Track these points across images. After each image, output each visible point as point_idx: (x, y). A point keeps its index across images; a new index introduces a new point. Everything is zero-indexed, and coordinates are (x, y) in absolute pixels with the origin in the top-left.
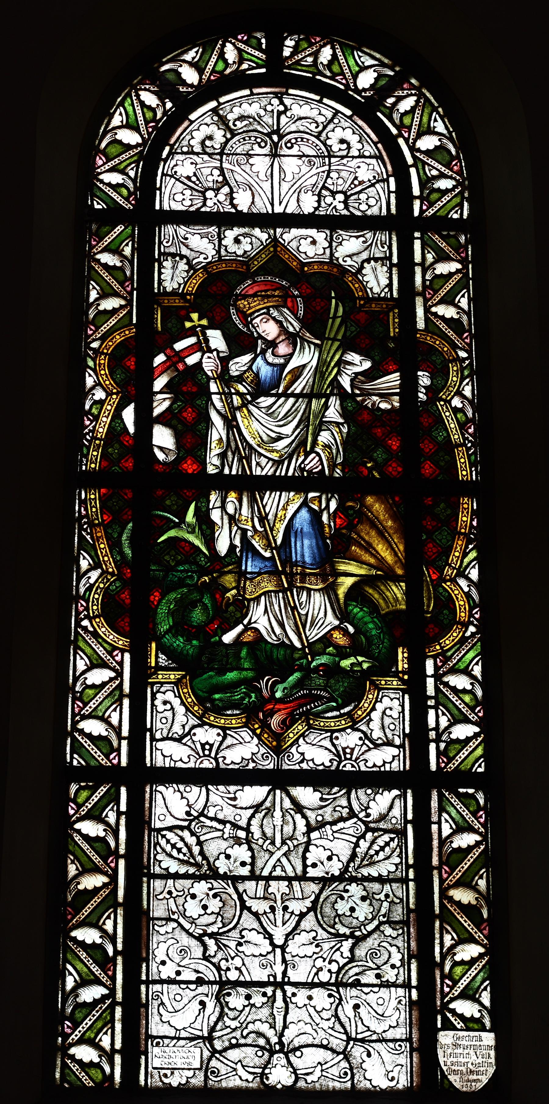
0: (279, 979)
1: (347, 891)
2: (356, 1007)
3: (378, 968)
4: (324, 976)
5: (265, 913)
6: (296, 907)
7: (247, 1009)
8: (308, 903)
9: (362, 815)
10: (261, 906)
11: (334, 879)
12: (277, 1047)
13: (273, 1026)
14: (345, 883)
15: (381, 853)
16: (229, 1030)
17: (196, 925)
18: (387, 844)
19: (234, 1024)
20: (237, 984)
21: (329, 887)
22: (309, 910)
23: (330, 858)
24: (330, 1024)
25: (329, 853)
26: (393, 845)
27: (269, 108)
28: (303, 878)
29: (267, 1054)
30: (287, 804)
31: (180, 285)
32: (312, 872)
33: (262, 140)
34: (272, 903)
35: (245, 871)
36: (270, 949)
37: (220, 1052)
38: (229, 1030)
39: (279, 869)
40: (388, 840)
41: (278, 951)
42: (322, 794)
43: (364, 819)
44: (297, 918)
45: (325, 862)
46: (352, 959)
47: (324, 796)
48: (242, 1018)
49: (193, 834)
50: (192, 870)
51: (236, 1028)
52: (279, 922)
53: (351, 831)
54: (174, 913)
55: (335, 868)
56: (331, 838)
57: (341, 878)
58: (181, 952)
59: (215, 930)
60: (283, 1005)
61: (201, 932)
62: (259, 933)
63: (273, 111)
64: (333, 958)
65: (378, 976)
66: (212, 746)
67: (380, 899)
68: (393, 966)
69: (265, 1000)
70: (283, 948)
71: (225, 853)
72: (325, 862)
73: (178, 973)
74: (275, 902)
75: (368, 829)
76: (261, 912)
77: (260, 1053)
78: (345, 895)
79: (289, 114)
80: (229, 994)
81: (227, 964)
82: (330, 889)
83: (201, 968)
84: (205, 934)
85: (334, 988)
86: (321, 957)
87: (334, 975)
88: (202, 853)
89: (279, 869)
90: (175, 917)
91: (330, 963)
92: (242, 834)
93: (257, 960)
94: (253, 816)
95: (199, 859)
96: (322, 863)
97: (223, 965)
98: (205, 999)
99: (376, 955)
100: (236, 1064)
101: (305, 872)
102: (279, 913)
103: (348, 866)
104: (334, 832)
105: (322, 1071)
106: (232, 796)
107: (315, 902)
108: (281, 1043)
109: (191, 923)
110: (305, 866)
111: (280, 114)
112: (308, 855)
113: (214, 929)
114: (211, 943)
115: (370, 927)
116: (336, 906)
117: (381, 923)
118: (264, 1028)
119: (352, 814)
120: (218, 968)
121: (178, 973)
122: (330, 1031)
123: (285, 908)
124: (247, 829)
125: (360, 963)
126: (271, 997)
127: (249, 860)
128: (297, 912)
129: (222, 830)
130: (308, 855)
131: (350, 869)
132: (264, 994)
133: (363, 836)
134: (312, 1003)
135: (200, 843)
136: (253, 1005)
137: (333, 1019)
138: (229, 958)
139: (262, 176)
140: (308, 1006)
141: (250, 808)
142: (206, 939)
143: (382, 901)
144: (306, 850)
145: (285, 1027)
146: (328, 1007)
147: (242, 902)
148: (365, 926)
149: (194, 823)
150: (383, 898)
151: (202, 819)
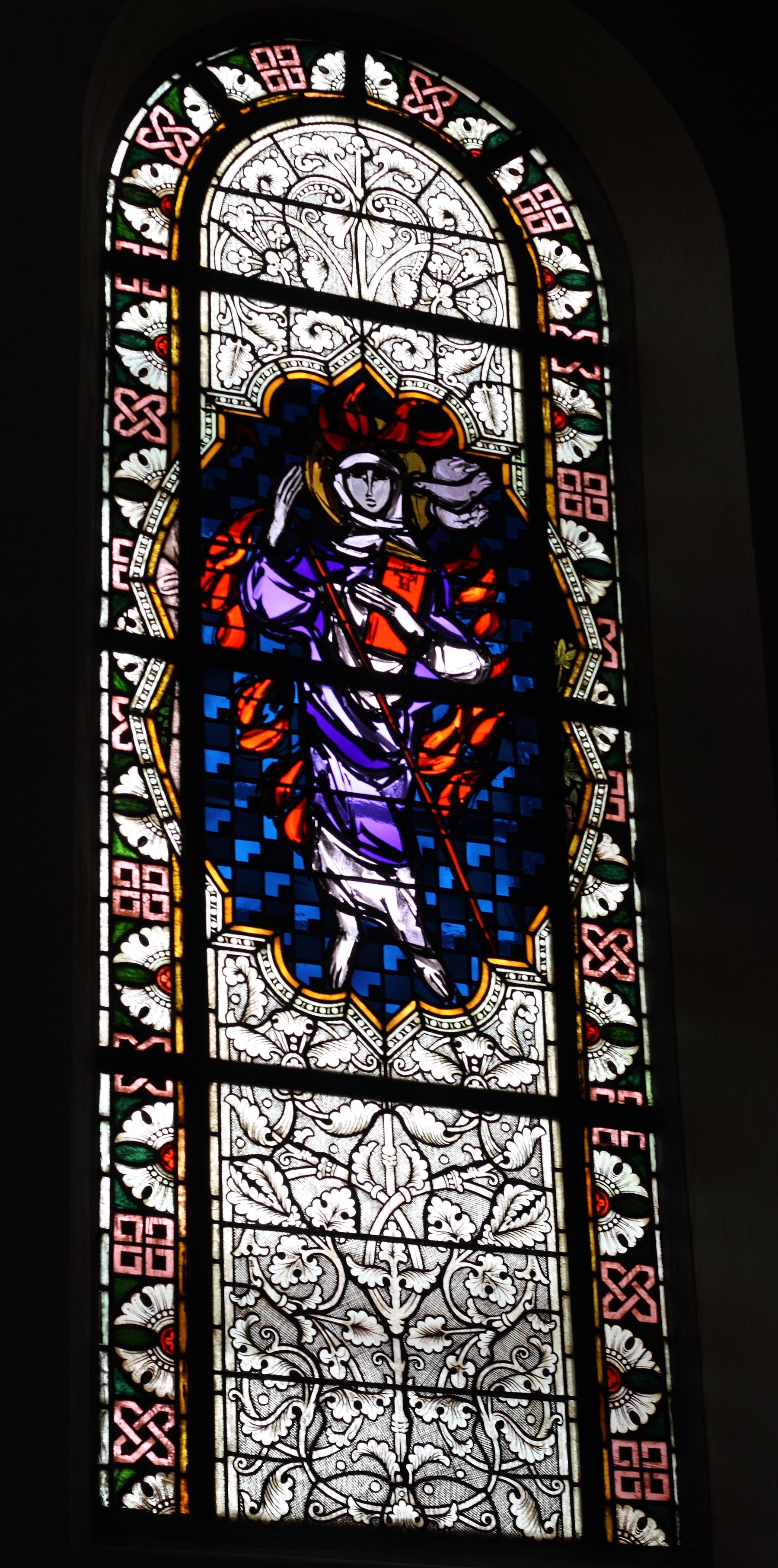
0: (399, 1380)
2: (499, 1425)
3: (529, 1372)
4: (458, 1381)
5: (377, 1286)
6: (419, 1283)
7: (358, 1421)
8: (432, 1277)
9: (498, 1160)
10: (372, 1277)
11: (463, 1245)
12: (399, 1479)
14: (480, 1252)
15: (525, 1215)
16: (334, 1449)
17: (288, 1297)
18: (533, 1204)
19: (341, 1440)
20: (343, 1385)
21: (459, 1255)
22: (434, 1287)
23: (458, 1217)
24: (466, 1449)
25: (457, 1210)
26: (540, 1205)
27: (350, 149)
28: (424, 1242)
29: (386, 1487)
31: (243, 380)
32: (435, 1235)
34: (388, 1276)
35: (347, 1226)
36: (385, 1338)
37: (325, 1481)
38: (334, 1449)
39: (392, 1225)
40: (532, 1198)
41: (396, 1343)
42: (447, 1126)
45: (453, 1220)
46: (491, 1360)
48: (352, 1432)
49: (278, 1168)
50: (276, 1220)
51: (344, 1446)
52: (396, 1303)
53: (484, 1182)
54: (256, 1278)
55: (465, 1229)
57: (473, 1245)
58: (266, 1333)
60: (405, 1420)
61: (294, 1308)
62: (369, 1314)
64: (470, 1357)
65: (527, 1384)
67: (523, 1279)
68: (546, 1372)
69: (380, 1410)
71: (320, 1198)
72: (453, 1220)
74: (389, 1272)
75: (508, 1181)
76: (372, 1285)
80: (332, 1400)
81: (330, 1356)
83: (297, 1360)
84: (299, 1311)
85: (469, 1398)
87: (470, 1379)
89: (392, 1225)
90: (258, 1283)
91: (465, 1361)
93: (368, 1353)
94: (356, 1149)
95: (287, 1203)
96: (447, 1222)
97: (325, 1356)
98: (300, 1405)
99: (524, 1354)
100: (347, 1497)
101: (427, 1233)
102: (395, 1288)
103: (483, 1229)
104: (464, 1181)
105: (459, 1513)
106: (326, 1117)
107: (440, 1278)
108: (403, 1472)
109: (281, 1294)
110: (426, 1224)
111: (364, 160)
112: (430, 1208)
113: (310, 1304)
114: (307, 1324)
115: (513, 1316)
118: (381, 1450)
120: (318, 1361)
121: (264, 1364)
123: (402, 1283)
124: (348, 1167)
126: (388, 1407)
127: (352, 1212)
129: (316, 1166)
130: (430, 1208)
131: (485, 1234)
132: (380, 1403)
133: (500, 1189)
135: (286, 1182)
137: (470, 1442)
138: (332, 1349)
139: (339, 242)
141: (355, 1134)
142: (301, 1318)
144: (428, 1203)
146: (464, 1425)
147: (347, 1269)
149: (278, 1152)
150: (528, 1277)
151: (288, 1146)
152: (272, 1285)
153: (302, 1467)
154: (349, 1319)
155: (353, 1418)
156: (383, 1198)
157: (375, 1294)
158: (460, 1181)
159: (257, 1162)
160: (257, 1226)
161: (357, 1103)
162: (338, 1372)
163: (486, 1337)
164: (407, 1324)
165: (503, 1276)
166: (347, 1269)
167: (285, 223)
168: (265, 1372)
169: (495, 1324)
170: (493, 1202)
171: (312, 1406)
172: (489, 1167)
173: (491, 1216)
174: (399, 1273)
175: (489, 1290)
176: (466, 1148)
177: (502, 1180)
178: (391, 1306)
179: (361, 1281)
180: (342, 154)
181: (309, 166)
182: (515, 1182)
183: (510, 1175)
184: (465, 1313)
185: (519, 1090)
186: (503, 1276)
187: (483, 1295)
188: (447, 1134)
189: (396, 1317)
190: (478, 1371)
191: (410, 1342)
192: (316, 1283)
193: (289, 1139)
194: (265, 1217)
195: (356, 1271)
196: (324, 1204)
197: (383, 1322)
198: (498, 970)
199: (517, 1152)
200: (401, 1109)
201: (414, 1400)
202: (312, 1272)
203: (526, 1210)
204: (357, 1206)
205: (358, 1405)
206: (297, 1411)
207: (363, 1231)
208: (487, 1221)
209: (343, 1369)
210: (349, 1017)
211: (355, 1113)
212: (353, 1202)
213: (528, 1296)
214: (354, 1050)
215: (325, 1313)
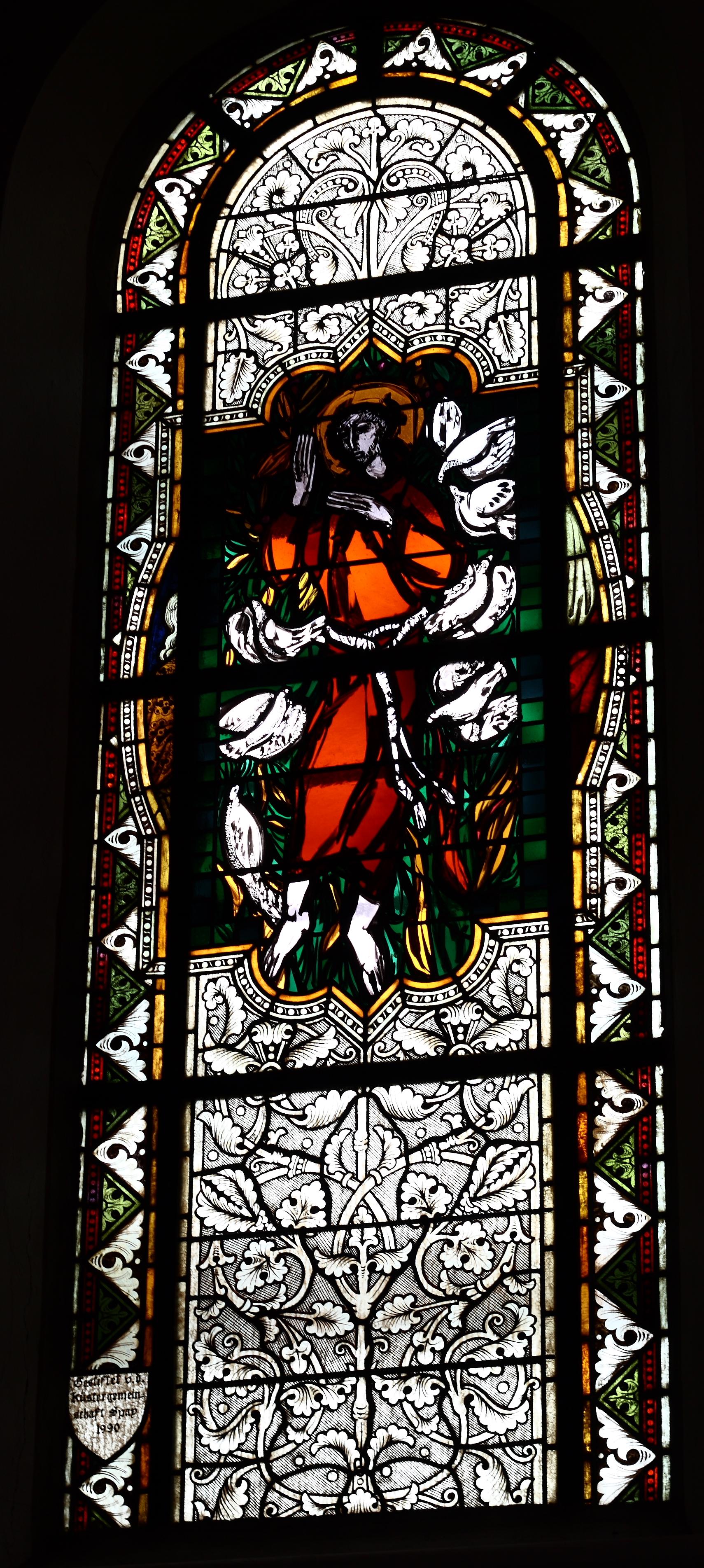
0: (361, 1366)
1: (457, 1233)
2: (468, 1400)
4: (426, 1358)
6: (387, 1263)
7: (318, 1414)
8: (404, 1256)
11: (439, 1218)
13: (352, 1436)
14: (455, 1223)
18: (516, 1161)
21: (434, 1229)
22: (404, 1265)
23: (433, 1190)
25: (433, 1183)
26: (524, 1162)
30: (376, 1116)
33: (350, 180)
35: (319, 1220)
36: (351, 1326)
40: (517, 1156)
41: (361, 1329)
43: (485, 1128)
44: (387, 1279)
46: (463, 1331)
47: (428, 1101)
49: (249, 1174)
50: (243, 1227)
53: (463, 1149)
55: (441, 1202)
56: (438, 1161)
59: (276, 1306)
63: (370, 136)
65: (500, 1351)
66: (277, 1047)
68: (522, 1336)
69: (342, 1398)
70: (367, 1323)
73: (226, 1372)
74: (358, 1259)
75: (490, 1143)
76: (338, 1274)
77: (333, 1476)
78: (455, 1239)
79: (393, 135)
82: (438, 1230)
86: (421, 1330)
88: (260, 1200)
92: (314, 1167)
95: (256, 1208)
97: (286, 1353)
99: (498, 1320)
100: (301, 1494)
107: (412, 1255)
110: (400, 1203)
112: (404, 1186)
114: (272, 1324)
115: (489, 1282)
116: (443, 1257)
117: (503, 1275)
119: (468, 1124)
120: (279, 1360)
121: (226, 1372)
122: (434, 1436)
123: (372, 1268)
124: (320, 1160)
125: (475, 1335)
126: (350, 1394)
127: (322, 1204)
128: (388, 1270)
129: (288, 1167)
130: (404, 1186)
132: (341, 1392)
133: (482, 1153)
134: (410, 1397)
135: (257, 1188)
136: (327, 1408)
138: (295, 1345)
139: (351, 232)
140: (405, 1404)
143: (507, 1244)
144: (404, 1180)
145: (371, 1434)
147: (314, 1262)
148: (481, 1280)
150: (508, 1239)
151: (260, 1152)
152: (238, 1292)
153: (259, 1468)
154: (314, 1312)
155: (314, 1411)
156: (354, 1185)
157: (342, 1285)
158: (437, 1152)
159: (228, 1172)
160: (226, 1235)
161: (334, 1093)
162: (299, 1367)
163: (457, 1309)
164: (375, 1307)
165: (481, 1242)
166: (314, 1262)
167: (296, 232)
168: (227, 1379)
169: (469, 1293)
170: (473, 1168)
171: (273, 1406)
172: (470, 1131)
173: (470, 1181)
174: (370, 1256)
175: (465, 1259)
176: (445, 1117)
177: (483, 1142)
178: (358, 1292)
179: (328, 1272)
180: (357, 140)
181: (323, 164)
182: (497, 1143)
183: (492, 1136)
184: (438, 1288)
185: (508, 1049)
186: (481, 1242)
187: (459, 1265)
188: (426, 1106)
189: (362, 1303)
190: (448, 1345)
191: (377, 1324)
192: (283, 1282)
193: (263, 1143)
194: (235, 1226)
195: (323, 1263)
196: (293, 1202)
197: (348, 1308)
198: (491, 928)
199: (500, 1110)
200: (379, 1091)
201: (379, 1383)
202: (278, 1272)
203: (510, 1169)
204: (328, 1198)
205: (319, 1398)
206: (257, 1415)
207: (334, 1222)
208: (466, 1188)
209: (305, 1362)
210: (330, 1013)
211: (333, 1103)
212: (323, 1194)
213: (506, 1259)
214: (333, 1044)
215: (292, 1309)
